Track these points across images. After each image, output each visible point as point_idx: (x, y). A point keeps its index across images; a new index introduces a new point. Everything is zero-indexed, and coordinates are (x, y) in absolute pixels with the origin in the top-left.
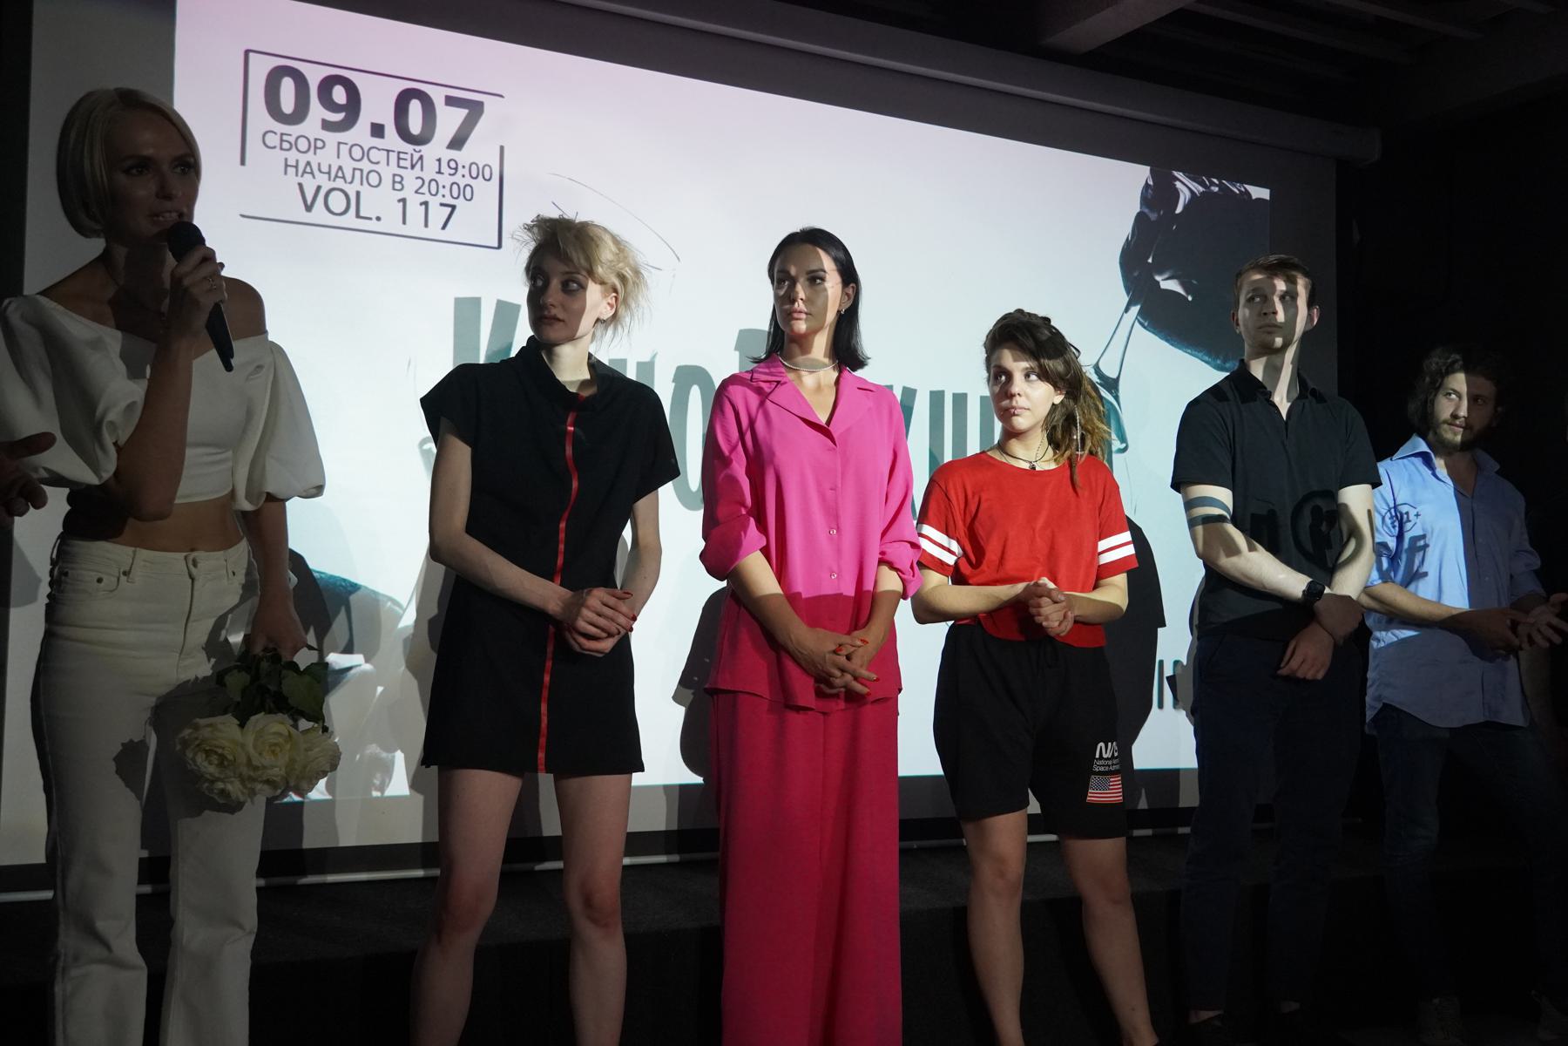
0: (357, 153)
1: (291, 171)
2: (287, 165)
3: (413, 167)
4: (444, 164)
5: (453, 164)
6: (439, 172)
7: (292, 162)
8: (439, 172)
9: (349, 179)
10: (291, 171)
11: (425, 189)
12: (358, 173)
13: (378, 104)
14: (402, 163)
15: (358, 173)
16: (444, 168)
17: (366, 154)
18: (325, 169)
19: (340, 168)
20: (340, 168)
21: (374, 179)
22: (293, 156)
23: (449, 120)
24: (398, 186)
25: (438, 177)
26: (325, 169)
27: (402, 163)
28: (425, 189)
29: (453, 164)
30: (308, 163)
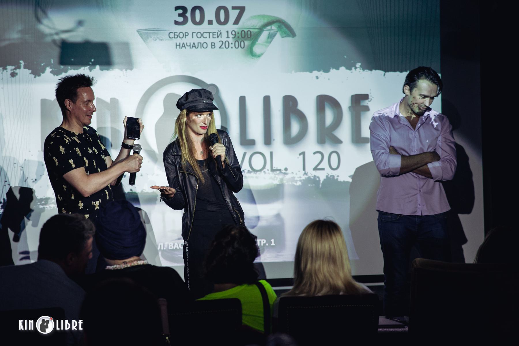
0: (199, 35)
1: (178, 47)
2: (176, 45)
6: (228, 37)
7: (178, 44)
10: (178, 47)
11: (223, 46)
12: (199, 44)
14: (214, 36)
15: (199, 44)
17: (202, 35)
18: (188, 44)
19: (194, 43)
20: (194, 43)
21: (205, 45)
22: (179, 41)
24: (213, 47)
25: (228, 39)
26: (188, 44)
27: (214, 36)
28: (223, 46)
29: (234, 33)
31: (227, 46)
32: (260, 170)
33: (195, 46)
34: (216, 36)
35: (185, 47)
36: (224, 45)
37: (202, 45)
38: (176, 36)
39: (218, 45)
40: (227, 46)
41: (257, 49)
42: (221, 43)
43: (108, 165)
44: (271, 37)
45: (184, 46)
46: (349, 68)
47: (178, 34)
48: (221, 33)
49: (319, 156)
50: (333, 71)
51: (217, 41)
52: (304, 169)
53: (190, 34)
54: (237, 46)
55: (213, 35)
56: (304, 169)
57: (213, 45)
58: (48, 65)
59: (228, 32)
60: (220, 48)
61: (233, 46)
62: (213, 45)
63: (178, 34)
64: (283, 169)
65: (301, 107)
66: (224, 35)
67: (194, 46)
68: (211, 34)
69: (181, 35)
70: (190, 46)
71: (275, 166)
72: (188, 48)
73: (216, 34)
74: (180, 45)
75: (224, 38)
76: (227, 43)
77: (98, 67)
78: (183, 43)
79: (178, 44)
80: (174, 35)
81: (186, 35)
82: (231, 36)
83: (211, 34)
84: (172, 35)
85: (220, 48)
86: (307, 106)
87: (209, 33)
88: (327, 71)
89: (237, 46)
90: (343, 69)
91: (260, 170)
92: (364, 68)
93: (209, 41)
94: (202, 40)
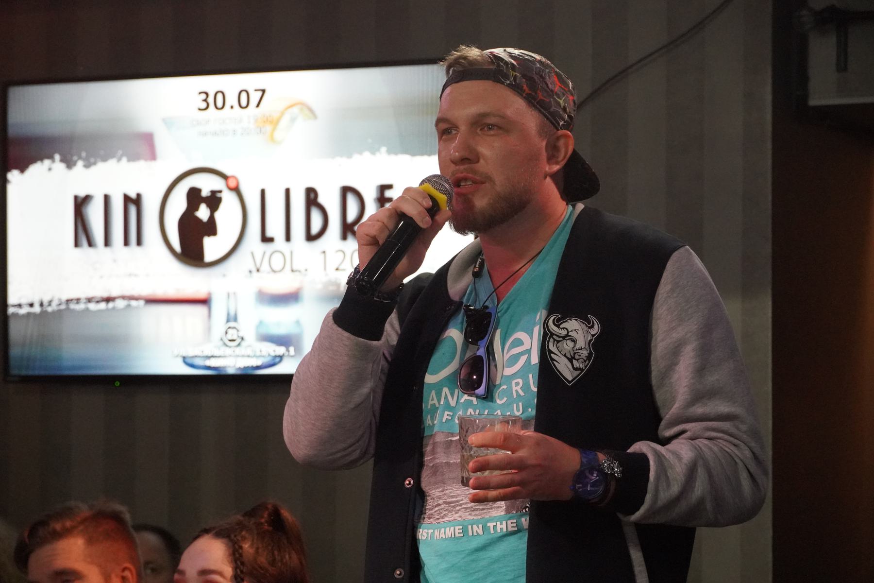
13: (232, 99)
23: (255, 97)
32: (280, 271)
41: (278, 135)
43: (208, 257)
44: (293, 120)
46: (373, 153)
49: (341, 254)
50: (356, 157)
52: (325, 269)
56: (325, 269)
58: (80, 158)
64: (303, 270)
65: (321, 200)
67: (215, 134)
71: (295, 268)
77: (124, 159)
86: (330, 200)
88: (349, 156)
90: (367, 154)
91: (280, 271)
92: (390, 152)
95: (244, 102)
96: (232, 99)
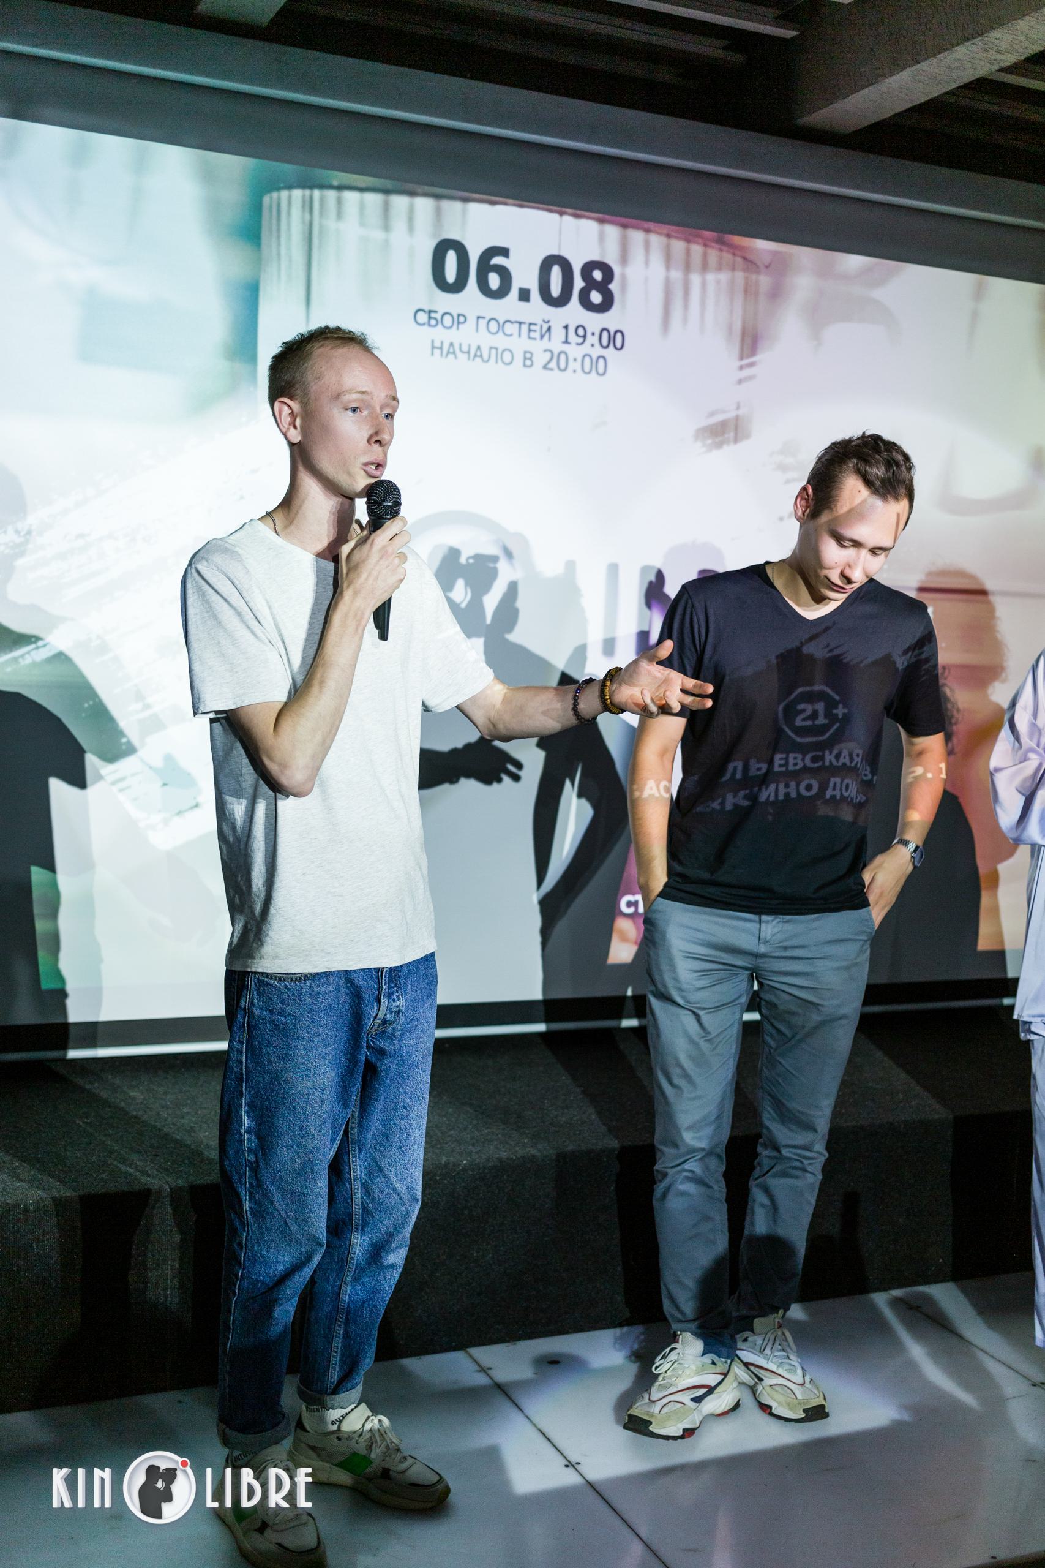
1: (437, 352)
2: (433, 347)
3: (542, 337)
4: (572, 330)
5: (581, 332)
6: (566, 342)
7: (437, 344)
8: (566, 342)
9: (486, 357)
10: (437, 352)
11: (553, 364)
12: (493, 351)
15: (493, 351)
16: (572, 337)
17: (501, 326)
18: (465, 349)
19: (479, 348)
20: (479, 348)
21: (507, 357)
22: (439, 334)
24: (528, 363)
25: (565, 347)
26: (465, 349)
27: (533, 334)
28: (553, 364)
29: (581, 332)
30: (451, 344)
31: (563, 366)
33: (481, 356)
34: (537, 335)
35: (454, 353)
36: (556, 361)
37: (500, 355)
38: (433, 322)
39: (541, 358)
40: (563, 366)
42: (548, 355)
45: (451, 350)
47: (438, 316)
48: (549, 329)
51: (538, 348)
53: (472, 320)
54: (587, 369)
55: (530, 330)
57: (528, 358)
59: (566, 327)
60: (545, 367)
61: (577, 366)
62: (528, 358)
63: (438, 316)
66: (558, 334)
67: (478, 354)
68: (525, 328)
69: (447, 320)
70: (468, 352)
72: (463, 357)
73: (537, 328)
74: (441, 348)
75: (556, 345)
76: (563, 357)
78: (451, 344)
79: (437, 344)
80: (430, 318)
81: (460, 319)
82: (572, 337)
83: (525, 328)
84: (422, 317)
85: (545, 367)
87: (520, 323)
89: (587, 369)
93: (519, 343)
94: (500, 341)
95: (556, 290)
96: (525, 275)
